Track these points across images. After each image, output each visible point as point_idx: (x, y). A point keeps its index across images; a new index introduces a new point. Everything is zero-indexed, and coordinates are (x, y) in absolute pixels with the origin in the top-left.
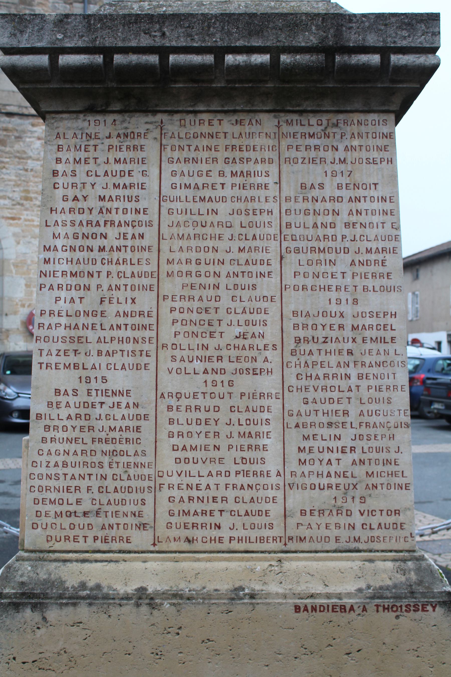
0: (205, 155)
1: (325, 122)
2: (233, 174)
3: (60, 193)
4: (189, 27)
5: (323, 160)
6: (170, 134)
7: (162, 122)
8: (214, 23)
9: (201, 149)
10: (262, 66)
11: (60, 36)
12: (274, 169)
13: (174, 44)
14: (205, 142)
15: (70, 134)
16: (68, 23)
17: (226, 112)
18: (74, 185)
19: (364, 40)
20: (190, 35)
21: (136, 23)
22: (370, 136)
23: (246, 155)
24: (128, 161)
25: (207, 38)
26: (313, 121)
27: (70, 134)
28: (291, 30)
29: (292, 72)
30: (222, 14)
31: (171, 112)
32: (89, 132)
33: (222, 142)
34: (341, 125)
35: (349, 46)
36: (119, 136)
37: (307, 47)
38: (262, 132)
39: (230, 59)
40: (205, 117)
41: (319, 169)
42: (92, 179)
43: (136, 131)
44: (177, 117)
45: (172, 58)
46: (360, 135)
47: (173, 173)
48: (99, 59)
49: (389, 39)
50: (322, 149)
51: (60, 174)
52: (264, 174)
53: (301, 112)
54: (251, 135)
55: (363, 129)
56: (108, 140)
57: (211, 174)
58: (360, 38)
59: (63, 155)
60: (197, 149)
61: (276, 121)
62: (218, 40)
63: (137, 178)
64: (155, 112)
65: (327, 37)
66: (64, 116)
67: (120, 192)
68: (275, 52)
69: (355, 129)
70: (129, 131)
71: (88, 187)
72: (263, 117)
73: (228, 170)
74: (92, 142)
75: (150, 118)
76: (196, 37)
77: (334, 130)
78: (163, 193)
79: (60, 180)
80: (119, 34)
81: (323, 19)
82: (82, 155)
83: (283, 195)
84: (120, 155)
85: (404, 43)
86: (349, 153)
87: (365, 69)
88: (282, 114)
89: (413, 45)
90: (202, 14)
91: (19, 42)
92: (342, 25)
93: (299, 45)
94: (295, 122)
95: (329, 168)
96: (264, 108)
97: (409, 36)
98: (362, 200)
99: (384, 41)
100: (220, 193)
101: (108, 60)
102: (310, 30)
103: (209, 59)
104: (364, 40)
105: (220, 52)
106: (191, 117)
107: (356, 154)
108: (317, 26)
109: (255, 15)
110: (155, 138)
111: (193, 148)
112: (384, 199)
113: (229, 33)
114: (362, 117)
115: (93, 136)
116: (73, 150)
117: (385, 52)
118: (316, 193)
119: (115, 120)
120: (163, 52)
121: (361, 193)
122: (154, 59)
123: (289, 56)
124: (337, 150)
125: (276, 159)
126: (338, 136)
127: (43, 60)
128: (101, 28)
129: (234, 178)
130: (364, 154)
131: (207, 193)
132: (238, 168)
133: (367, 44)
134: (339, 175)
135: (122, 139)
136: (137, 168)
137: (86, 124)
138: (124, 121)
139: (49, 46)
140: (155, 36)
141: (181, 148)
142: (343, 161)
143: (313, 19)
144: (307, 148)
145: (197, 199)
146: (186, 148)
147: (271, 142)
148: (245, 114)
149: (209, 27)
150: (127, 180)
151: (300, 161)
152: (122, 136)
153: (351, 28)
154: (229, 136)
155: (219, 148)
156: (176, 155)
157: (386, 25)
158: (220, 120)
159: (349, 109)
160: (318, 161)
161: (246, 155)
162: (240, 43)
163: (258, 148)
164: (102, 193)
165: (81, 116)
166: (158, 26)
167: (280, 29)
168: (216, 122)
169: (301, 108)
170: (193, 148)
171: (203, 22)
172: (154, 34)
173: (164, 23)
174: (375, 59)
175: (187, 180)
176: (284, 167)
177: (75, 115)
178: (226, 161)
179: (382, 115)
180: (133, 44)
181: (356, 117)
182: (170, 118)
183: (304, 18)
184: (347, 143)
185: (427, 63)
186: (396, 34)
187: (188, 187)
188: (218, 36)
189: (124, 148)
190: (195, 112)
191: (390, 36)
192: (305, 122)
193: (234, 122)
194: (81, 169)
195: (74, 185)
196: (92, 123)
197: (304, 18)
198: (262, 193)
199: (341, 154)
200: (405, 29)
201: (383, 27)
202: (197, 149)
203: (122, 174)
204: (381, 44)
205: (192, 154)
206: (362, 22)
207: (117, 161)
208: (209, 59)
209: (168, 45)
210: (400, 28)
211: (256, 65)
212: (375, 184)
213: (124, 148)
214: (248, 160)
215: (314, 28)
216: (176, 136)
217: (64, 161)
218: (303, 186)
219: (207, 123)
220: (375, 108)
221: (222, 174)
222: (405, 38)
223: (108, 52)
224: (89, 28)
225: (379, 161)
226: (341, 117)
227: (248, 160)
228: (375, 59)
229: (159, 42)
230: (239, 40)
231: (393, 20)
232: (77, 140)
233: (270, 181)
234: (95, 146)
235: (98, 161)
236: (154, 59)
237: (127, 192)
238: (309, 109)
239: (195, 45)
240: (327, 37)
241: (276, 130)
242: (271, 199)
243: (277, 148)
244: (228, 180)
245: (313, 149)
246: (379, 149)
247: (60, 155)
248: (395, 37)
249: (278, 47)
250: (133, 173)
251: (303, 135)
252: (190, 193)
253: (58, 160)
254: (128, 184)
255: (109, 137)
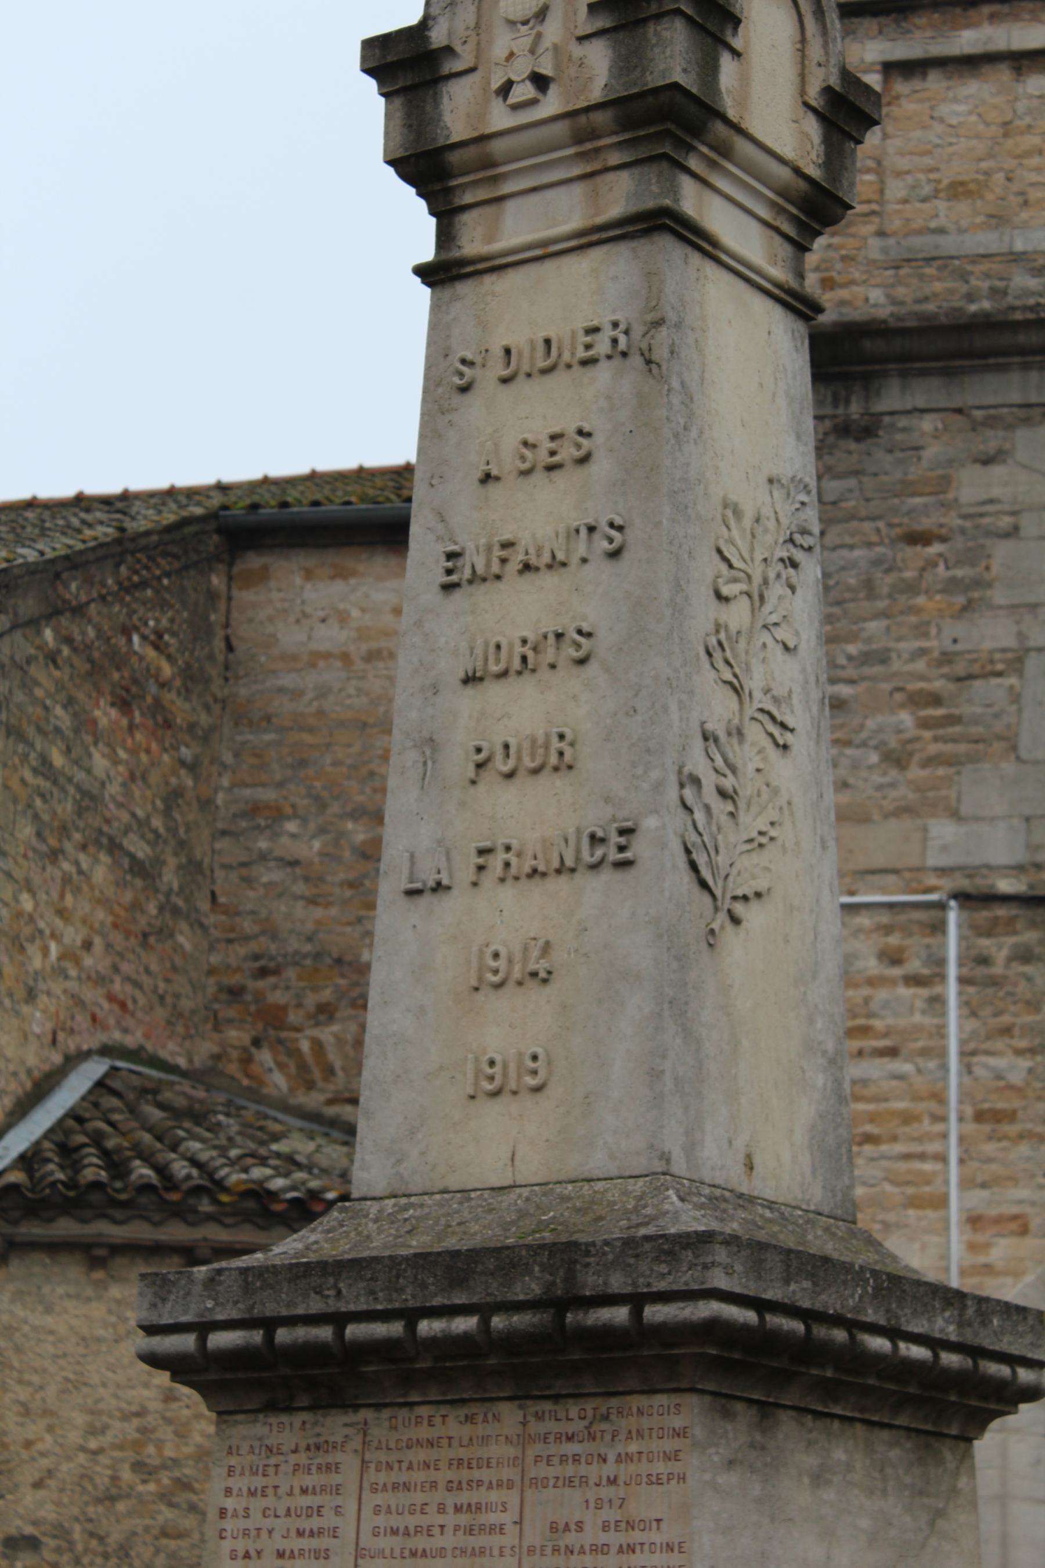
0: (419, 1476)
1: (590, 1413)
2: (458, 1509)
3: (227, 1545)
4: (371, 1279)
5: (584, 1480)
6: (375, 1444)
7: (366, 1423)
8: (405, 1270)
9: (415, 1466)
10: (466, 1338)
11: (210, 1304)
12: (513, 1498)
13: (352, 1307)
14: (421, 1455)
15: (245, 1448)
16: (220, 1283)
17: (452, 1402)
18: (246, 1533)
19: (605, 1283)
20: (372, 1292)
21: (305, 1276)
22: (654, 1435)
23: (476, 1474)
24: (318, 1490)
25: (395, 1295)
26: (573, 1412)
27: (245, 1448)
28: (506, 1274)
29: (511, 1344)
30: (416, 1255)
31: (378, 1407)
32: (268, 1442)
33: (446, 1454)
34: (613, 1417)
35: (585, 1297)
36: (308, 1448)
37: (528, 1301)
38: (500, 1433)
39: (426, 1327)
40: (424, 1411)
41: (576, 1496)
42: (268, 1523)
43: (331, 1439)
44: (386, 1413)
45: (353, 1331)
46: (640, 1434)
47: (377, 1510)
48: (257, 1337)
49: (641, 1280)
50: (583, 1460)
51: (229, 1514)
52: (500, 1508)
53: (556, 1398)
54: (485, 1440)
55: (645, 1422)
56: (293, 1456)
57: (427, 1509)
58: (600, 1281)
59: (239, 1483)
60: (410, 1467)
61: (521, 1413)
62: (408, 1298)
63: (329, 1520)
64: (356, 1407)
65: (554, 1283)
66: (240, 1417)
67: (305, 1543)
68: (484, 1311)
69: (633, 1422)
70: (322, 1439)
71: (264, 1534)
72: (505, 1408)
73: (450, 1500)
74: (273, 1461)
75: (351, 1417)
76: (380, 1294)
77: (604, 1426)
78: (362, 1545)
79: (229, 1524)
80: (283, 1296)
81: (551, 1252)
82: (259, 1482)
83: (526, 1544)
84: (309, 1481)
85: (661, 1286)
86: (622, 1466)
87: (607, 1333)
88: (529, 1402)
89: (675, 1288)
90: (390, 1257)
91: (160, 1316)
92: (576, 1261)
93: (516, 1298)
94: (547, 1415)
95: (591, 1494)
96: (502, 1395)
97: (669, 1273)
98: (638, 1549)
99: (634, 1284)
100: (439, 1541)
101: (269, 1337)
102: (529, 1272)
103: (396, 1329)
104: (605, 1283)
105: (411, 1316)
106: (403, 1413)
107: (632, 1468)
108: (541, 1265)
109: (458, 1253)
110: (356, 1451)
111: (405, 1465)
112: (670, 1548)
113: (424, 1286)
114: (643, 1401)
115: (275, 1450)
116: (247, 1473)
117: (637, 1301)
118: (571, 1538)
119: (304, 1423)
120: (339, 1320)
121: (637, 1536)
122: (325, 1333)
123: (504, 1317)
124: (605, 1461)
125: (517, 1479)
126: (608, 1437)
127: (187, 1342)
128: (261, 1288)
129: (459, 1515)
130: (644, 1468)
131: (420, 1542)
132: (465, 1497)
133: (610, 1291)
134: (606, 1506)
135: (311, 1454)
136: (328, 1501)
137: (266, 1429)
138: (315, 1424)
139: (197, 1320)
140: (328, 1296)
141: (389, 1466)
142: (613, 1481)
143: (536, 1254)
144: (563, 1459)
145: (407, 1553)
146: (396, 1466)
147: (512, 1451)
148: (478, 1404)
149: (398, 1277)
150: (315, 1523)
151: (552, 1482)
152: (312, 1448)
153: (588, 1265)
154: (455, 1443)
155: (441, 1464)
156: (382, 1477)
157: (637, 1256)
158: (444, 1416)
159: (621, 1389)
160: (577, 1483)
161: (476, 1474)
162: (437, 1301)
163: (494, 1462)
164: (280, 1544)
165: (261, 1416)
166: (331, 1280)
167: (492, 1274)
168: (438, 1420)
169: (552, 1392)
170: (405, 1465)
171: (391, 1269)
172: (327, 1293)
173: (340, 1274)
174: (620, 1314)
175: (395, 1521)
176: (529, 1494)
177: (252, 1416)
178: (451, 1486)
179: (673, 1396)
180: (300, 1311)
181: (637, 1401)
182: (376, 1415)
183: (524, 1253)
184: (620, 1448)
185: (695, 1318)
186: (652, 1270)
187: (395, 1532)
188: (409, 1291)
189: (314, 1468)
190: (411, 1405)
191: (642, 1275)
192: (561, 1415)
193: (462, 1419)
194: (257, 1504)
195: (246, 1533)
196: (275, 1428)
197: (524, 1253)
198: (495, 1541)
199: (609, 1469)
200: (665, 1262)
201: (632, 1261)
202: (410, 1467)
203: (310, 1512)
204: (629, 1290)
205: (404, 1477)
206: (605, 1254)
207: (304, 1491)
208: (396, 1329)
209: (344, 1309)
210: (657, 1260)
211: (458, 1335)
212: (658, 1521)
213: (314, 1468)
214: (480, 1483)
215: (537, 1268)
216: (384, 1446)
217: (235, 1492)
218: (554, 1528)
219: (425, 1422)
220: (659, 1387)
221: (441, 1509)
222: (663, 1276)
223: (269, 1325)
224: (247, 1289)
225: (665, 1478)
226: (614, 1402)
227: (480, 1483)
228: (620, 1314)
229: (333, 1306)
230: (436, 1295)
231: (647, 1246)
232: (255, 1458)
233: (507, 1518)
234: (277, 1466)
235: (280, 1491)
236: (325, 1333)
237: (314, 1543)
238: (564, 1392)
239: (379, 1307)
240: (554, 1283)
241: (519, 1430)
242: (507, 1551)
243: (518, 1462)
244: (450, 1519)
245: (570, 1461)
246: (667, 1457)
247: (231, 1482)
248: (650, 1276)
249: (487, 1304)
250: (324, 1511)
251: (558, 1438)
252: (397, 1542)
253: (228, 1491)
254: (315, 1530)
255: (295, 1451)
